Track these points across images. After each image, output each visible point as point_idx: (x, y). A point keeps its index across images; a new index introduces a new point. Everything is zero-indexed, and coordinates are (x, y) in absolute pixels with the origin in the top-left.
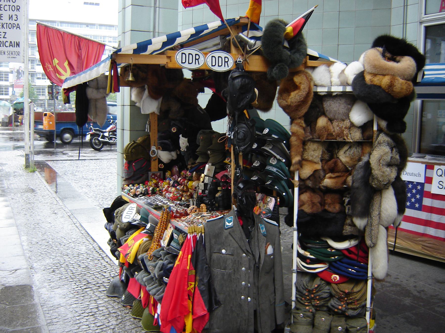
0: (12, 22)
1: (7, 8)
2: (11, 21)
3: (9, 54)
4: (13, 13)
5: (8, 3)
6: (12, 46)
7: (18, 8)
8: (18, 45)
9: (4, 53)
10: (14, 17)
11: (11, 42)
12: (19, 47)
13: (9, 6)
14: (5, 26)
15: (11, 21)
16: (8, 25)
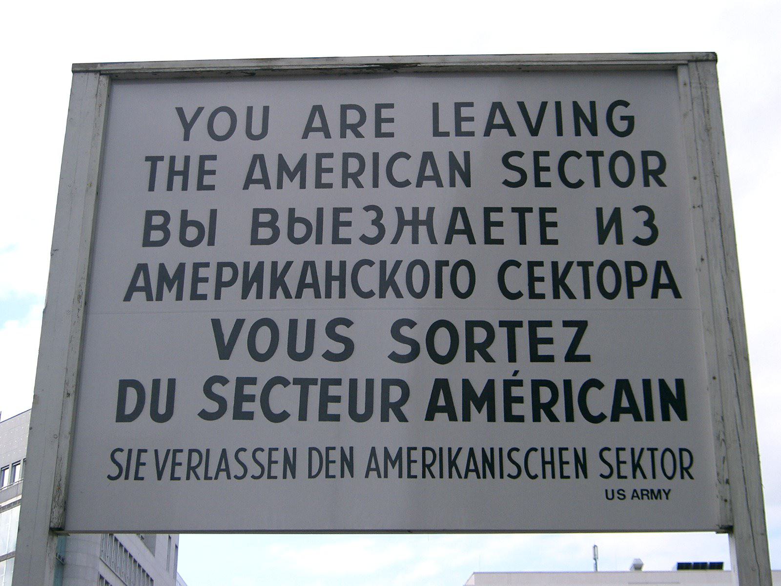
0: (621, 254)
1: (578, 169)
2: (610, 250)
3: (614, 471)
4: (626, 199)
5: (586, 142)
6: (633, 410)
7: (653, 163)
8: (675, 401)
9: (581, 464)
10: (633, 225)
11: (623, 386)
12: (683, 416)
13: (595, 155)
14: (574, 280)
15: (610, 250)
16: (593, 272)
